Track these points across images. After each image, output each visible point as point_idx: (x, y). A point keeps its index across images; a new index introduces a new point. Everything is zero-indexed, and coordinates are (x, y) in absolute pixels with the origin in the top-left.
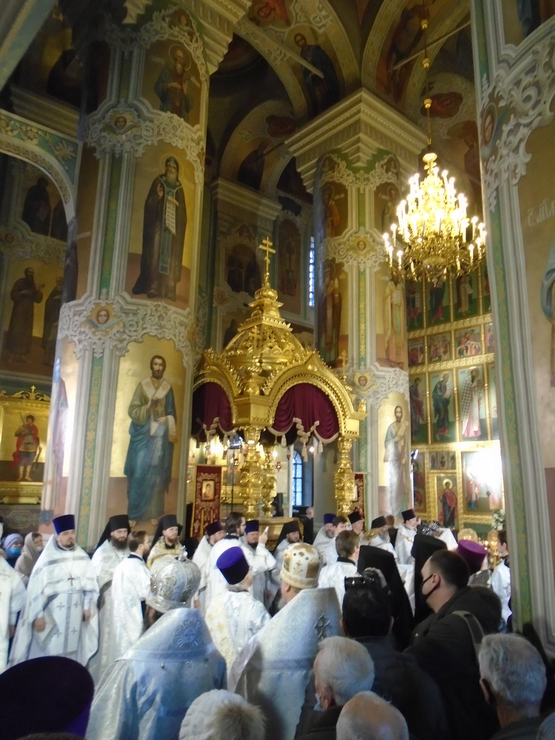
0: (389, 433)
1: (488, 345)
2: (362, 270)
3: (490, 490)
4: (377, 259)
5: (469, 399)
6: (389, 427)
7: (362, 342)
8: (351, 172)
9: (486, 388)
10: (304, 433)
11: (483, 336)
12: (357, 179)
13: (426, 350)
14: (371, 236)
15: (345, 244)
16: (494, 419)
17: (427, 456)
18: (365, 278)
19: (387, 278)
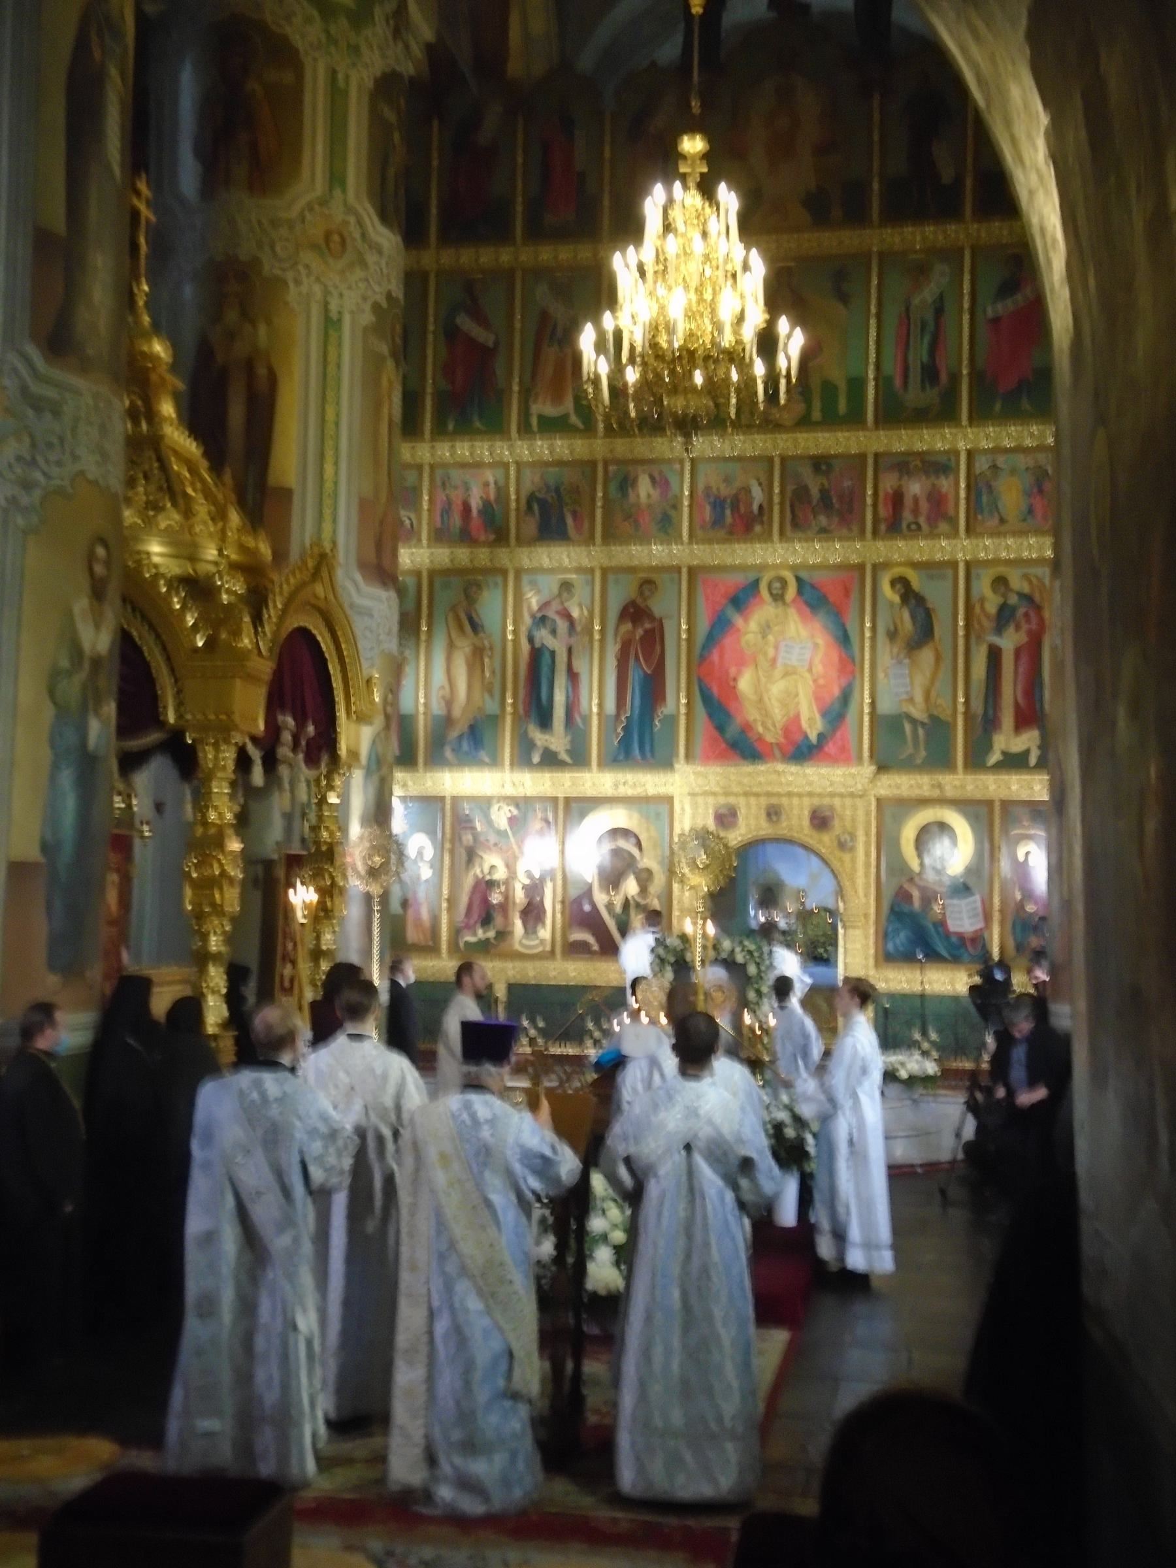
0: (373, 757)
1: (439, 525)
2: (334, 315)
3: (410, 896)
4: (369, 293)
6: (374, 742)
7: (327, 512)
8: (315, 13)
9: (423, 637)
10: (291, 755)
11: (426, 498)
12: (331, 40)
14: (360, 223)
15: (291, 227)
16: (435, 717)
18: (340, 337)
19: (384, 349)
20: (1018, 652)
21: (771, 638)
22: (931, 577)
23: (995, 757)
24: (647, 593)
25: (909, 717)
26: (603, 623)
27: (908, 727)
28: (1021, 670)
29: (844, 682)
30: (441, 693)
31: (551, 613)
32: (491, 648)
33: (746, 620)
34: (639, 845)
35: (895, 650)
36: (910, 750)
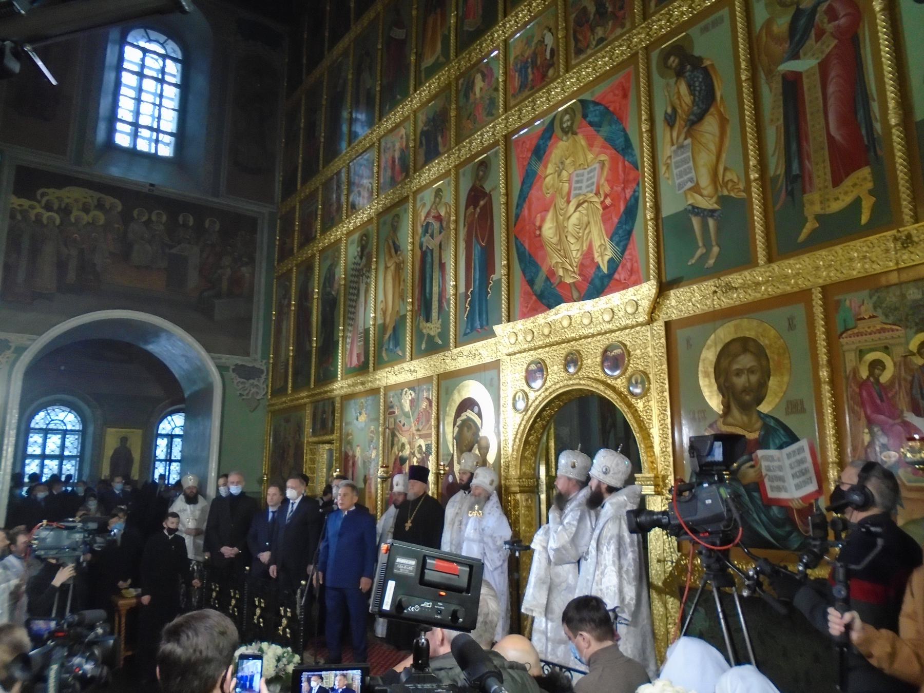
5: (356, 292)
13: (319, 212)
17: (309, 411)
20: (824, 67)
21: (564, 173)
22: (705, 29)
23: (811, 225)
24: (481, 173)
25: (695, 210)
26: (457, 214)
27: (696, 222)
28: (831, 89)
29: (629, 193)
30: (382, 306)
31: (431, 220)
32: (403, 262)
33: (546, 167)
34: (480, 415)
35: (675, 134)
36: (699, 252)
